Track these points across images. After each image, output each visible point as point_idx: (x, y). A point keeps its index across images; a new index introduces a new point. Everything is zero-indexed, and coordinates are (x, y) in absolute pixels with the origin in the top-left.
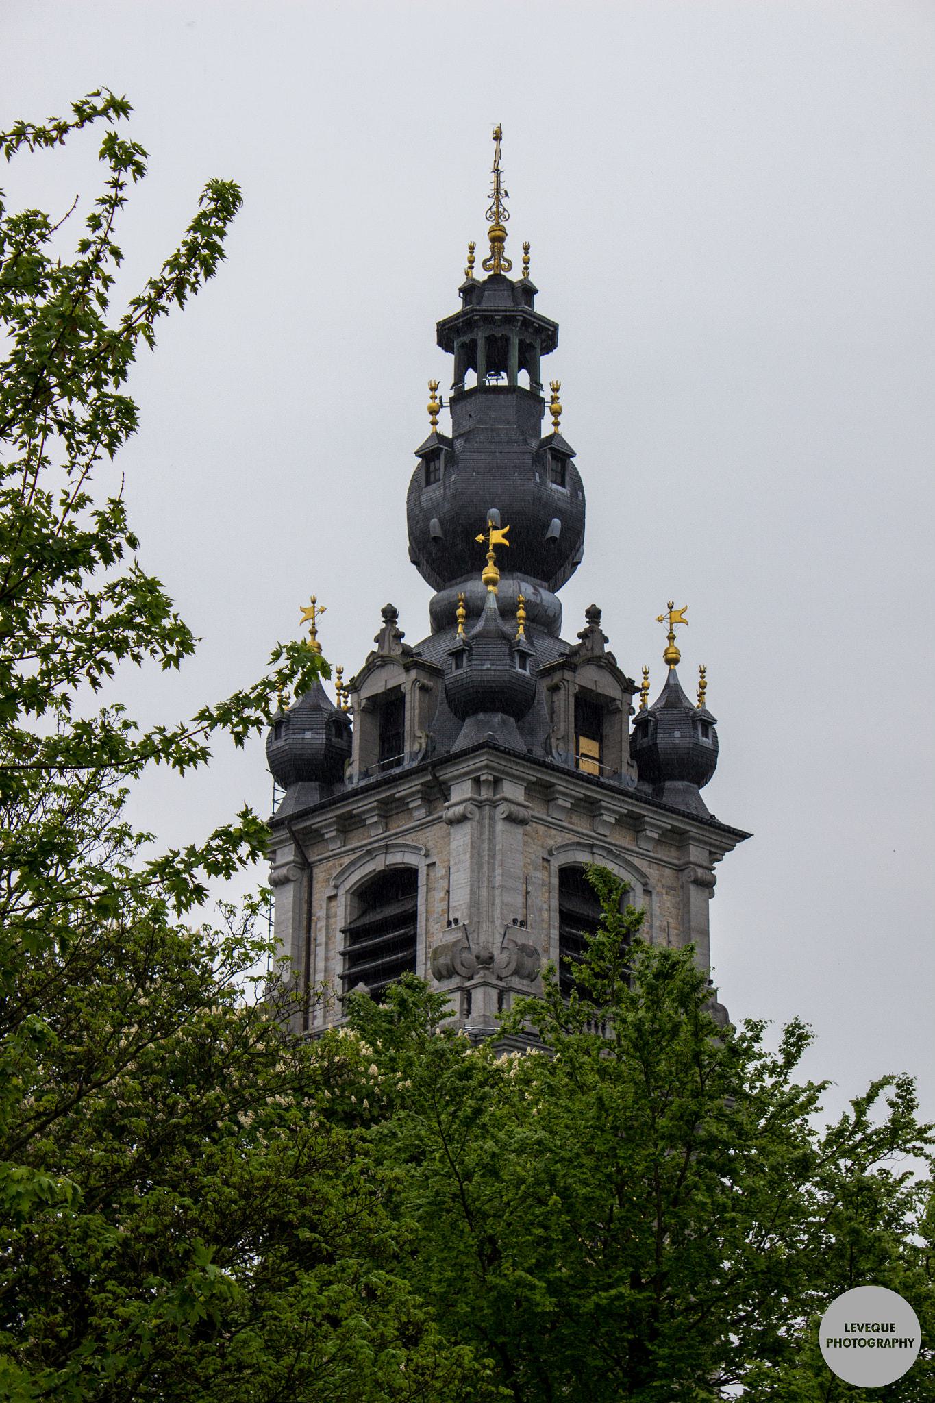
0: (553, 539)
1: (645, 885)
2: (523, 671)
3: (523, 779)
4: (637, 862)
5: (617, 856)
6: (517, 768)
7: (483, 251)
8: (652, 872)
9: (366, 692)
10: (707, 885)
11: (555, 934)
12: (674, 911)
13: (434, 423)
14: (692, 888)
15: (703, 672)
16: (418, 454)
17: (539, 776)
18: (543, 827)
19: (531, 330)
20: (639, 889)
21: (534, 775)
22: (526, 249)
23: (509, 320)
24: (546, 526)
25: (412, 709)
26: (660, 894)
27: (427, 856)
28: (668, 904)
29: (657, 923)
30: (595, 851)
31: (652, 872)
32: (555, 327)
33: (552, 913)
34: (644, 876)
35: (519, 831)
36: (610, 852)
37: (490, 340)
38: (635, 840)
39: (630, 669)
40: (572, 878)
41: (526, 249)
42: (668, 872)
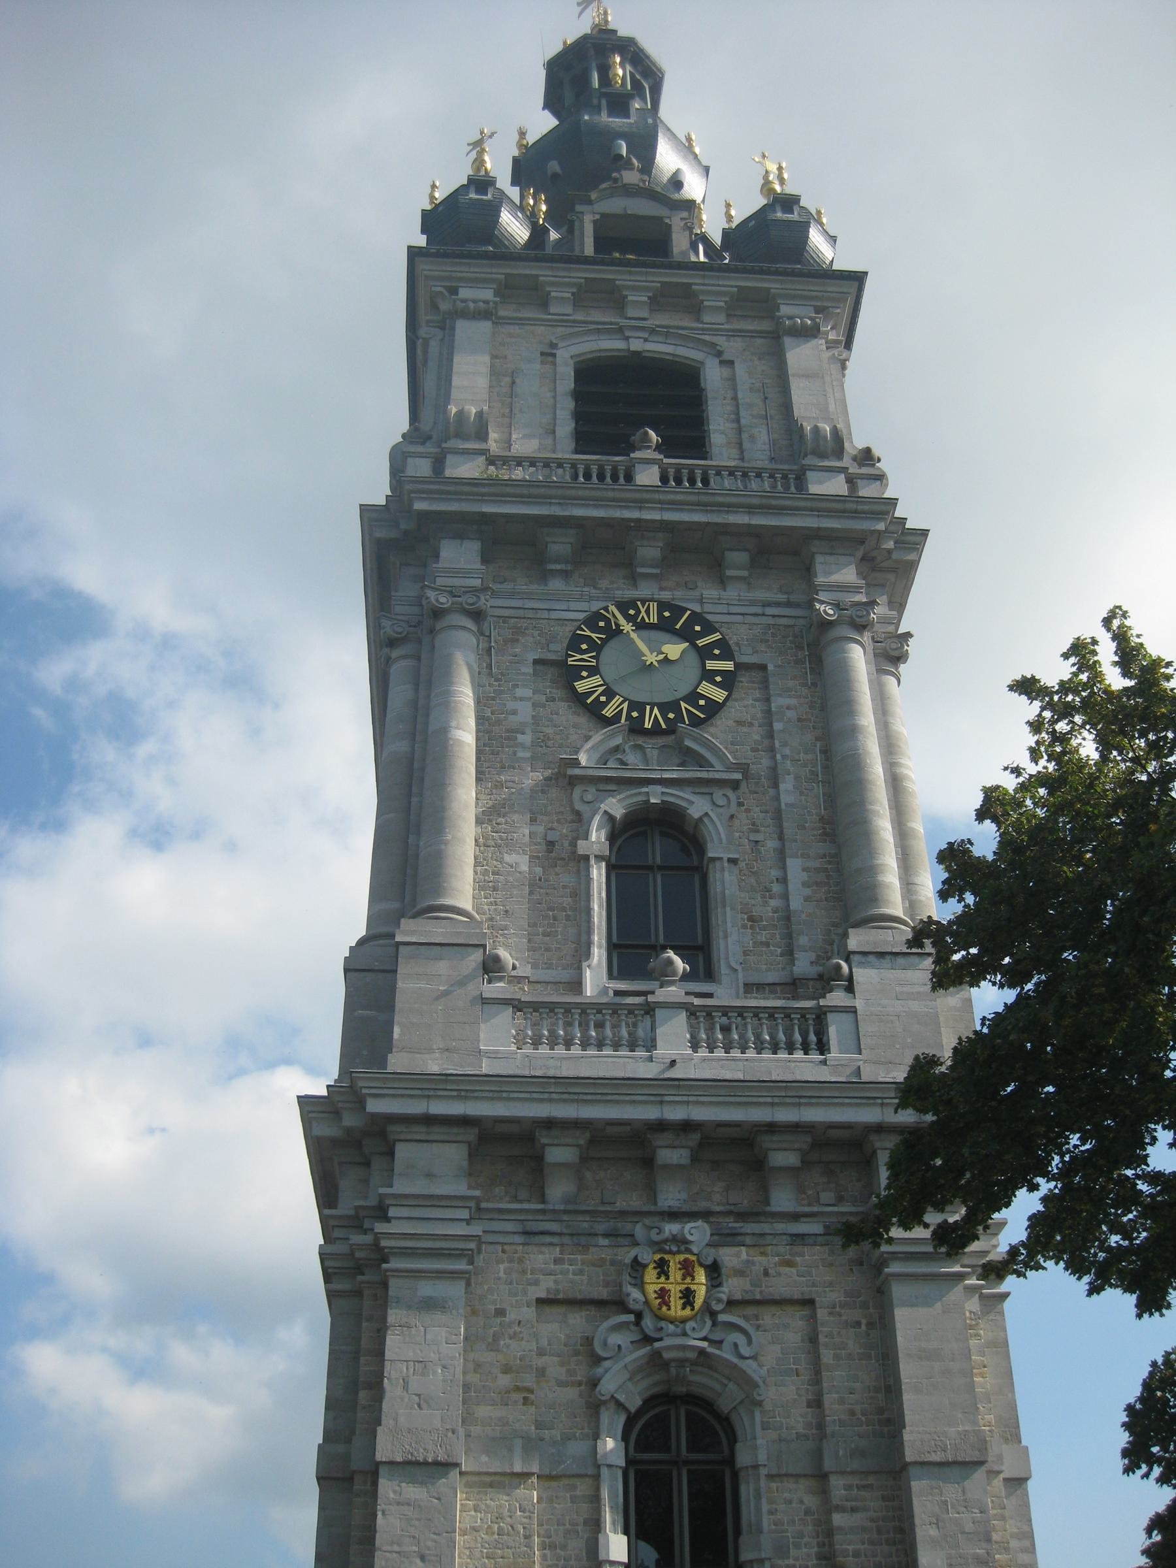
1: (719, 354)
2: (484, 197)
3: (485, 281)
5: (667, 335)
6: (472, 270)
8: (732, 347)
17: (508, 271)
18: (543, 328)
21: (500, 271)
30: (628, 333)
31: (732, 347)
33: (558, 398)
34: (713, 345)
35: (486, 326)
36: (652, 331)
38: (698, 320)
42: (759, 341)
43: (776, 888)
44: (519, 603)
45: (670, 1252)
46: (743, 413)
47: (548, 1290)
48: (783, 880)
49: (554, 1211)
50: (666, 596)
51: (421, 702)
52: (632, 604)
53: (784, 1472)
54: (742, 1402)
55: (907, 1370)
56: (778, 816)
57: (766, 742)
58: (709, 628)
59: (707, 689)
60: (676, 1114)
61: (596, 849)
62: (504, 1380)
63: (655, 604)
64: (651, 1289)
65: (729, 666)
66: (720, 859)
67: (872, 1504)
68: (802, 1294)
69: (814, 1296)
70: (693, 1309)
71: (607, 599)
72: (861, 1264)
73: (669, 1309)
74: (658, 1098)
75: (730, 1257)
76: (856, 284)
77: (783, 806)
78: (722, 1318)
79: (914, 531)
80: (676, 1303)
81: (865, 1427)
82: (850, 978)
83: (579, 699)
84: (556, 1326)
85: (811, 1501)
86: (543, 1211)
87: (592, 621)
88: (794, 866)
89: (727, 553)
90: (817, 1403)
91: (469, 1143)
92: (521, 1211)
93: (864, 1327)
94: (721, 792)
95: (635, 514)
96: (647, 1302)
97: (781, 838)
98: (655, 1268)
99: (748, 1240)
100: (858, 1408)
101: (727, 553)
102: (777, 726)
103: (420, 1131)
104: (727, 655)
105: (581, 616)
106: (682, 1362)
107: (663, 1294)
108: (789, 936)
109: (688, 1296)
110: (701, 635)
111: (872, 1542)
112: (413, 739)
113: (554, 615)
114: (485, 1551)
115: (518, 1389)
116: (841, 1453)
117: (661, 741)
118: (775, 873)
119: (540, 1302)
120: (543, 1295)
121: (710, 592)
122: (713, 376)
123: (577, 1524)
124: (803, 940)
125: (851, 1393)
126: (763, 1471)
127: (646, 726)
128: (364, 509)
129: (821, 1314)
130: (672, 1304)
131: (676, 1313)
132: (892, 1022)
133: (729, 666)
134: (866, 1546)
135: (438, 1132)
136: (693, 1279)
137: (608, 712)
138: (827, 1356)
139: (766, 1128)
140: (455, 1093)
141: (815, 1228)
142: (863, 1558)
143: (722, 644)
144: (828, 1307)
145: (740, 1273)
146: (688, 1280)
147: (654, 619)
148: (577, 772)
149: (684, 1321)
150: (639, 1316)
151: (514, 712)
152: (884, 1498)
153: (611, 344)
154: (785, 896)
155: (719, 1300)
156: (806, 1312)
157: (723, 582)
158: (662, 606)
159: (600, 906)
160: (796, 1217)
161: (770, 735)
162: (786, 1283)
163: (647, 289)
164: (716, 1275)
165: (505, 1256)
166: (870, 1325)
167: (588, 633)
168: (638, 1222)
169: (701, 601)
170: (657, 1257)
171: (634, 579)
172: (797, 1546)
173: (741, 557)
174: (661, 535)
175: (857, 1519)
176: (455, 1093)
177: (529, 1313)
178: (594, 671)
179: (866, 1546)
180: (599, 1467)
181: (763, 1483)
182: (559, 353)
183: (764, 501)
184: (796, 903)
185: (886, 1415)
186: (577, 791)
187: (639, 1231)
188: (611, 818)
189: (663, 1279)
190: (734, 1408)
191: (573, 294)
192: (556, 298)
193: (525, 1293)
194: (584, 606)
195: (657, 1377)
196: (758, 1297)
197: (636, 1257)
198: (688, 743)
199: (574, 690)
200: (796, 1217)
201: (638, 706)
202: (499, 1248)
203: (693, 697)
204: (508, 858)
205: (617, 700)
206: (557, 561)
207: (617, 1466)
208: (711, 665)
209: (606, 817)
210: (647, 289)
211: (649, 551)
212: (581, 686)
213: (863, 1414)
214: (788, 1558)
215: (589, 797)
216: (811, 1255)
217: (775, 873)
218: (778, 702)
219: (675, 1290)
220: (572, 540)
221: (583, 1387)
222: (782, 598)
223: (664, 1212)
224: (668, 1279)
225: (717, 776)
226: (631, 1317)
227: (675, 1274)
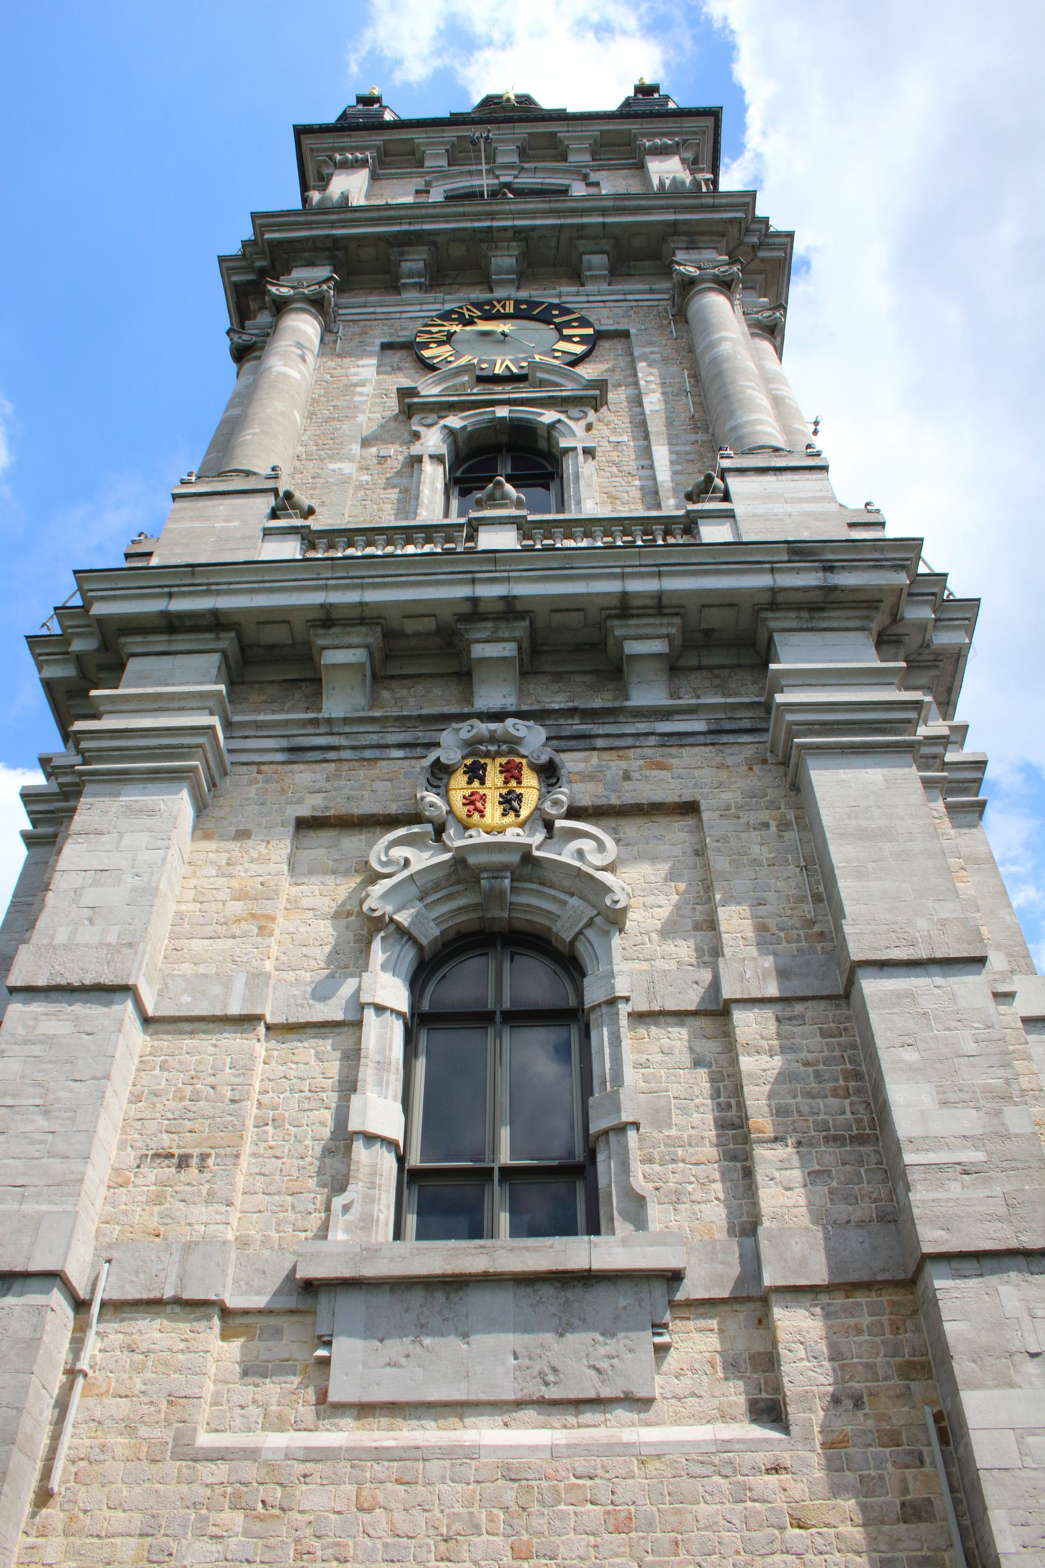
30: (497, 173)
44: (371, 310)
45: (487, 755)
47: (314, 808)
49: (329, 721)
50: (523, 294)
52: (490, 303)
53: (657, 1009)
54: (590, 923)
55: (839, 853)
57: (630, 380)
61: (433, 451)
62: (237, 907)
63: (512, 302)
64: (457, 798)
66: (574, 449)
67: (805, 1042)
68: (680, 796)
69: (698, 798)
70: (518, 816)
71: (459, 300)
72: (764, 762)
73: (483, 816)
74: (469, 576)
76: (709, 121)
77: (647, 412)
78: (559, 823)
79: (778, 234)
81: (784, 944)
84: (323, 851)
86: (315, 722)
89: (585, 258)
91: (224, 653)
92: (287, 723)
93: (773, 828)
94: (577, 410)
96: (450, 812)
98: (465, 773)
99: (600, 743)
100: (772, 923)
101: (585, 258)
103: (160, 642)
106: (498, 870)
109: (510, 802)
110: (556, 316)
111: (810, 1095)
114: (166, 1122)
115: (254, 916)
116: (749, 974)
119: (305, 825)
120: (305, 811)
123: (323, 1090)
125: (760, 904)
126: (624, 1009)
127: (497, 371)
128: (222, 260)
129: (705, 816)
130: (488, 812)
131: (493, 819)
132: (782, 520)
134: (799, 1099)
135: (182, 642)
136: (519, 782)
138: (720, 863)
139: (617, 611)
140: (204, 588)
141: (697, 725)
142: (796, 1117)
144: (718, 809)
145: (589, 777)
146: (513, 783)
150: (440, 830)
151: (356, 374)
152: (823, 1034)
155: (556, 803)
156: (690, 822)
158: (517, 303)
159: (434, 490)
164: (554, 781)
165: (260, 777)
166: (784, 826)
168: (443, 730)
169: (560, 296)
170: (468, 762)
171: (488, 285)
172: (685, 1111)
173: (599, 260)
174: (514, 244)
176: (204, 588)
179: (799, 1099)
180: (362, 1007)
181: (624, 1022)
182: (432, 191)
183: (618, 203)
185: (817, 928)
186: (416, 419)
188: (451, 432)
189: (476, 783)
190: (581, 932)
191: (447, 151)
192: (431, 154)
193: (282, 812)
194: (438, 306)
195: (462, 902)
196: (615, 801)
197: (439, 758)
202: (255, 768)
206: (410, 277)
207: (392, 1011)
209: (446, 431)
211: (504, 260)
213: (780, 929)
214: (669, 1126)
215: (429, 421)
216: (690, 756)
220: (424, 256)
221: (352, 918)
223: (482, 713)
224: (482, 782)
226: (429, 828)
227: (494, 777)
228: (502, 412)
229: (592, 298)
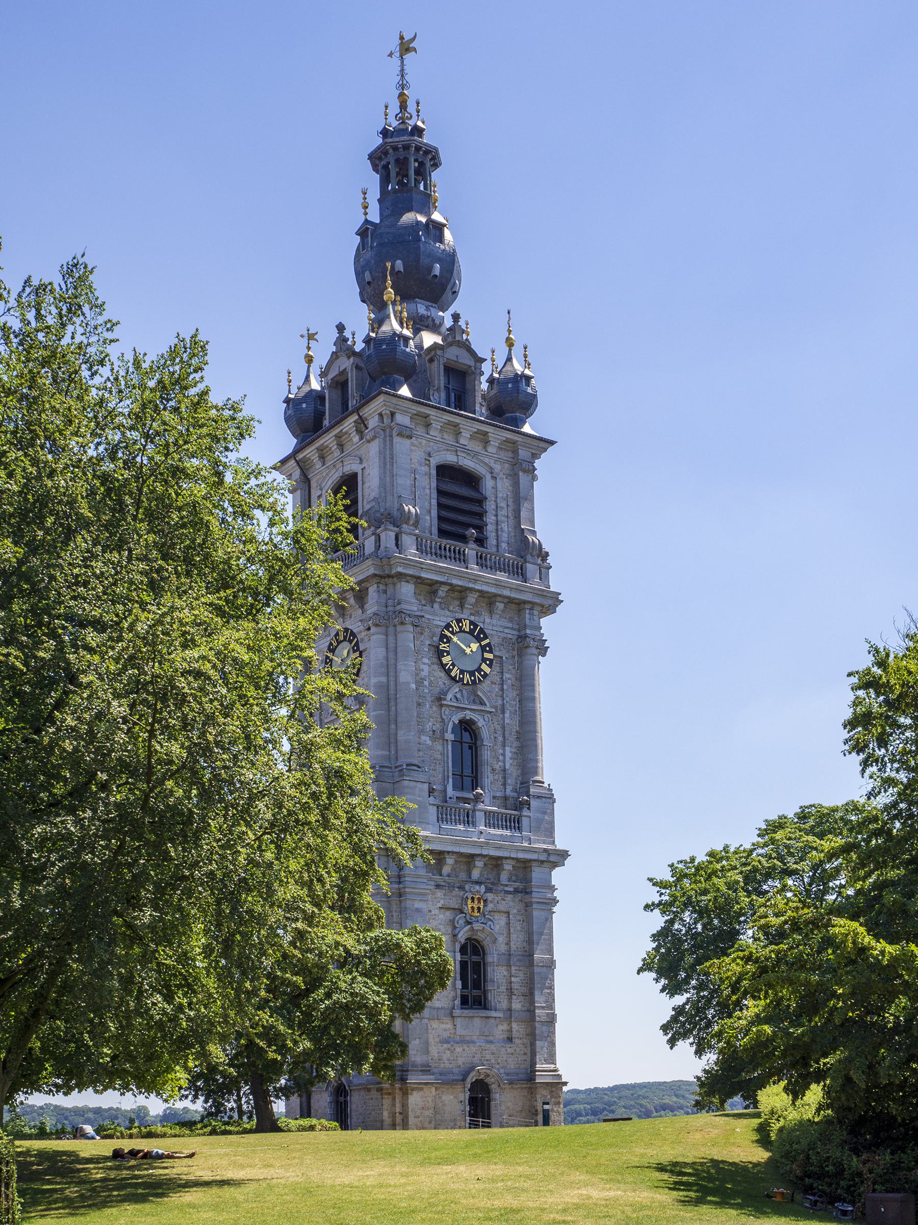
0: (436, 276)
4: (486, 460)
7: (394, 108)
9: (330, 376)
10: (531, 471)
11: (434, 502)
12: (511, 488)
13: (366, 214)
14: (521, 474)
15: (525, 348)
16: (357, 234)
19: (421, 153)
20: (488, 476)
22: (418, 103)
23: (406, 147)
24: (430, 269)
25: (352, 380)
26: (502, 479)
27: (361, 463)
28: (507, 484)
29: (500, 495)
32: (436, 149)
34: (492, 468)
37: (397, 161)
38: (485, 448)
39: (482, 351)
40: (445, 472)
41: (418, 103)
43: (501, 758)
46: (500, 513)
48: (504, 755)
50: (472, 618)
51: (392, 661)
56: (503, 727)
57: (500, 693)
58: (486, 637)
59: (484, 667)
60: (485, 852)
64: (469, 906)
65: (490, 656)
75: (490, 896)
80: (476, 911)
82: (529, 805)
83: (443, 666)
85: (505, 973)
87: (448, 626)
88: (508, 749)
90: (508, 944)
95: (471, 585)
97: (504, 737)
102: (505, 687)
104: (491, 651)
105: (444, 624)
107: (473, 908)
108: (504, 778)
109: (479, 908)
112: (388, 676)
113: (435, 622)
117: (467, 687)
118: (501, 751)
121: (488, 620)
122: (488, 485)
124: (509, 781)
133: (490, 656)
137: (453, 674)
138: (512, 931)
141: (512, 889)
143: (489, 645)
147: (467, 630)
148: (445, 702)
149: (477, 917)
153: (450, 458)
154: (504, 762)
157: (491, 612)
158: (471, 623)
160: (507, 886)
161: (502, 690)
162: (502, 906)
163: (470, 431)
167: (447, 633)
173: (501, 606)
175: (517, 979)
177: (437, 912)
178: (448, 653)
184: (507, 767)
187: (467, 887)
198: (479, 693)
199: (441, 661)
200: (507, 886)
201: (462, 672)
203: (479, 670)
204: (423, 738)
205: (456, 668)
208: (487, 655)
210: (470, 431)
212: (446, 660)
216: (510, 897)
217: (501, 751)
218: (506, 676)
219: (476, 906)
222: (510, 625)
225: (488, 709)
227: (476, 902)
228: (469, 715)
229: (495, 628)
